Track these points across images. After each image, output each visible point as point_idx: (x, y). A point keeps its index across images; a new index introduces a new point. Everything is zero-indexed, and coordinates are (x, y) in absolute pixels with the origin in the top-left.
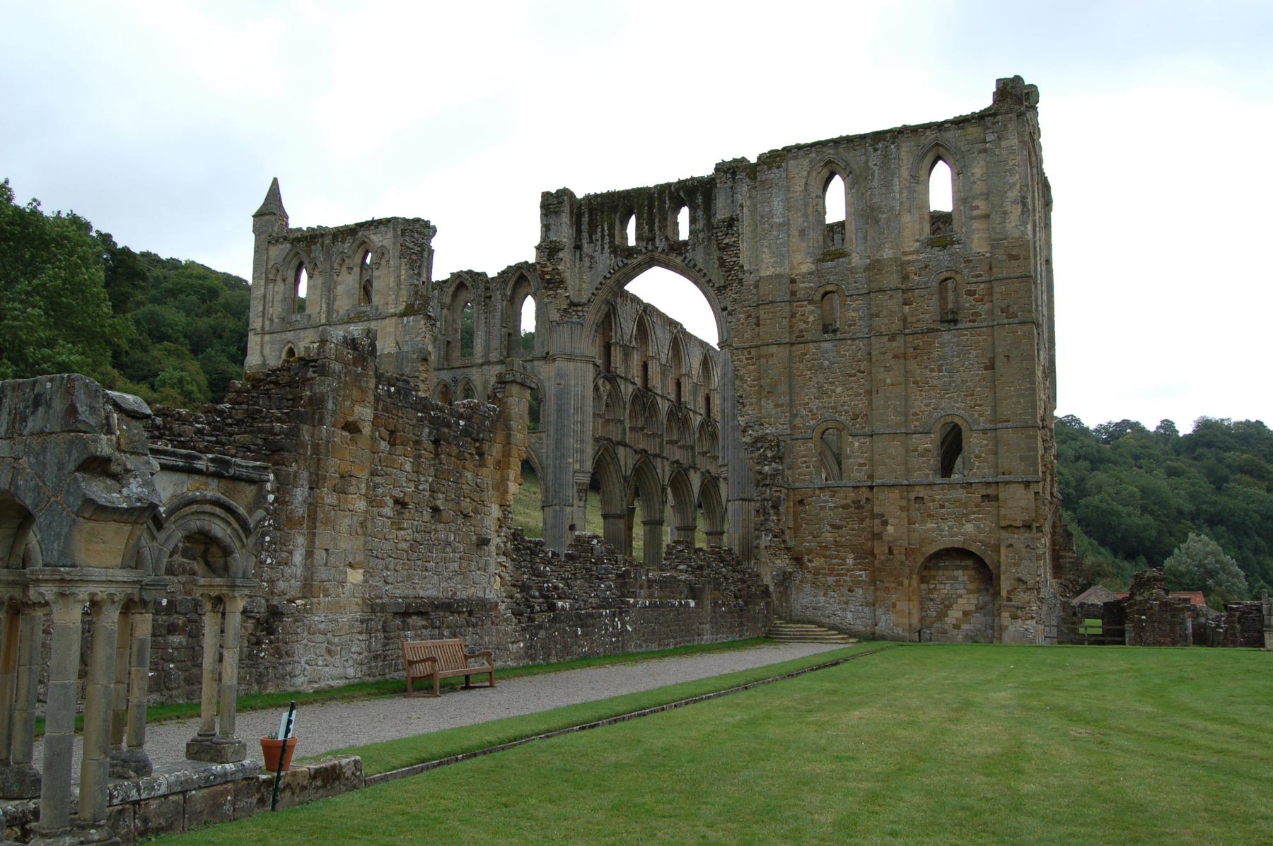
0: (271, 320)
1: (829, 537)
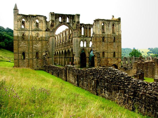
1: (103, 63)
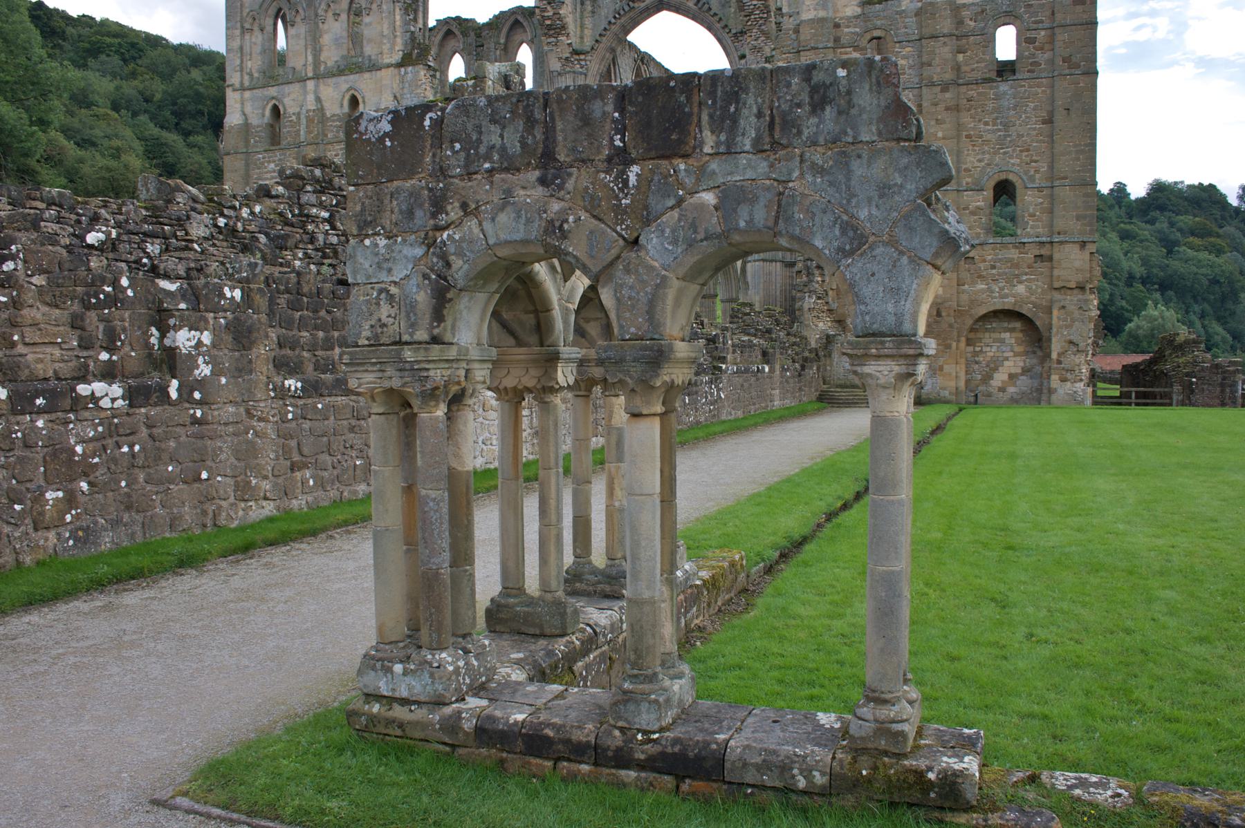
0: (251, 74)
